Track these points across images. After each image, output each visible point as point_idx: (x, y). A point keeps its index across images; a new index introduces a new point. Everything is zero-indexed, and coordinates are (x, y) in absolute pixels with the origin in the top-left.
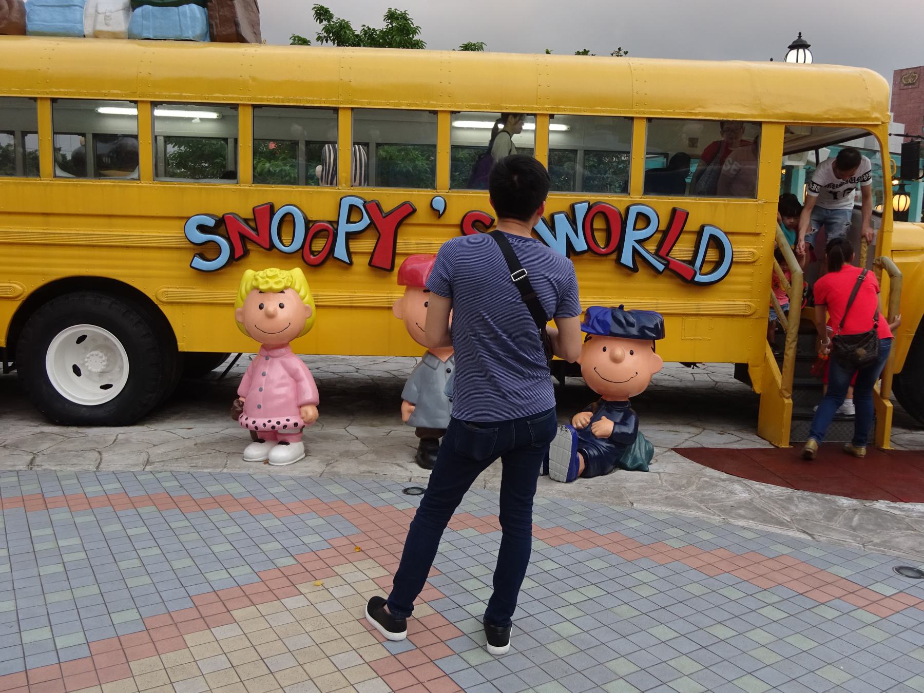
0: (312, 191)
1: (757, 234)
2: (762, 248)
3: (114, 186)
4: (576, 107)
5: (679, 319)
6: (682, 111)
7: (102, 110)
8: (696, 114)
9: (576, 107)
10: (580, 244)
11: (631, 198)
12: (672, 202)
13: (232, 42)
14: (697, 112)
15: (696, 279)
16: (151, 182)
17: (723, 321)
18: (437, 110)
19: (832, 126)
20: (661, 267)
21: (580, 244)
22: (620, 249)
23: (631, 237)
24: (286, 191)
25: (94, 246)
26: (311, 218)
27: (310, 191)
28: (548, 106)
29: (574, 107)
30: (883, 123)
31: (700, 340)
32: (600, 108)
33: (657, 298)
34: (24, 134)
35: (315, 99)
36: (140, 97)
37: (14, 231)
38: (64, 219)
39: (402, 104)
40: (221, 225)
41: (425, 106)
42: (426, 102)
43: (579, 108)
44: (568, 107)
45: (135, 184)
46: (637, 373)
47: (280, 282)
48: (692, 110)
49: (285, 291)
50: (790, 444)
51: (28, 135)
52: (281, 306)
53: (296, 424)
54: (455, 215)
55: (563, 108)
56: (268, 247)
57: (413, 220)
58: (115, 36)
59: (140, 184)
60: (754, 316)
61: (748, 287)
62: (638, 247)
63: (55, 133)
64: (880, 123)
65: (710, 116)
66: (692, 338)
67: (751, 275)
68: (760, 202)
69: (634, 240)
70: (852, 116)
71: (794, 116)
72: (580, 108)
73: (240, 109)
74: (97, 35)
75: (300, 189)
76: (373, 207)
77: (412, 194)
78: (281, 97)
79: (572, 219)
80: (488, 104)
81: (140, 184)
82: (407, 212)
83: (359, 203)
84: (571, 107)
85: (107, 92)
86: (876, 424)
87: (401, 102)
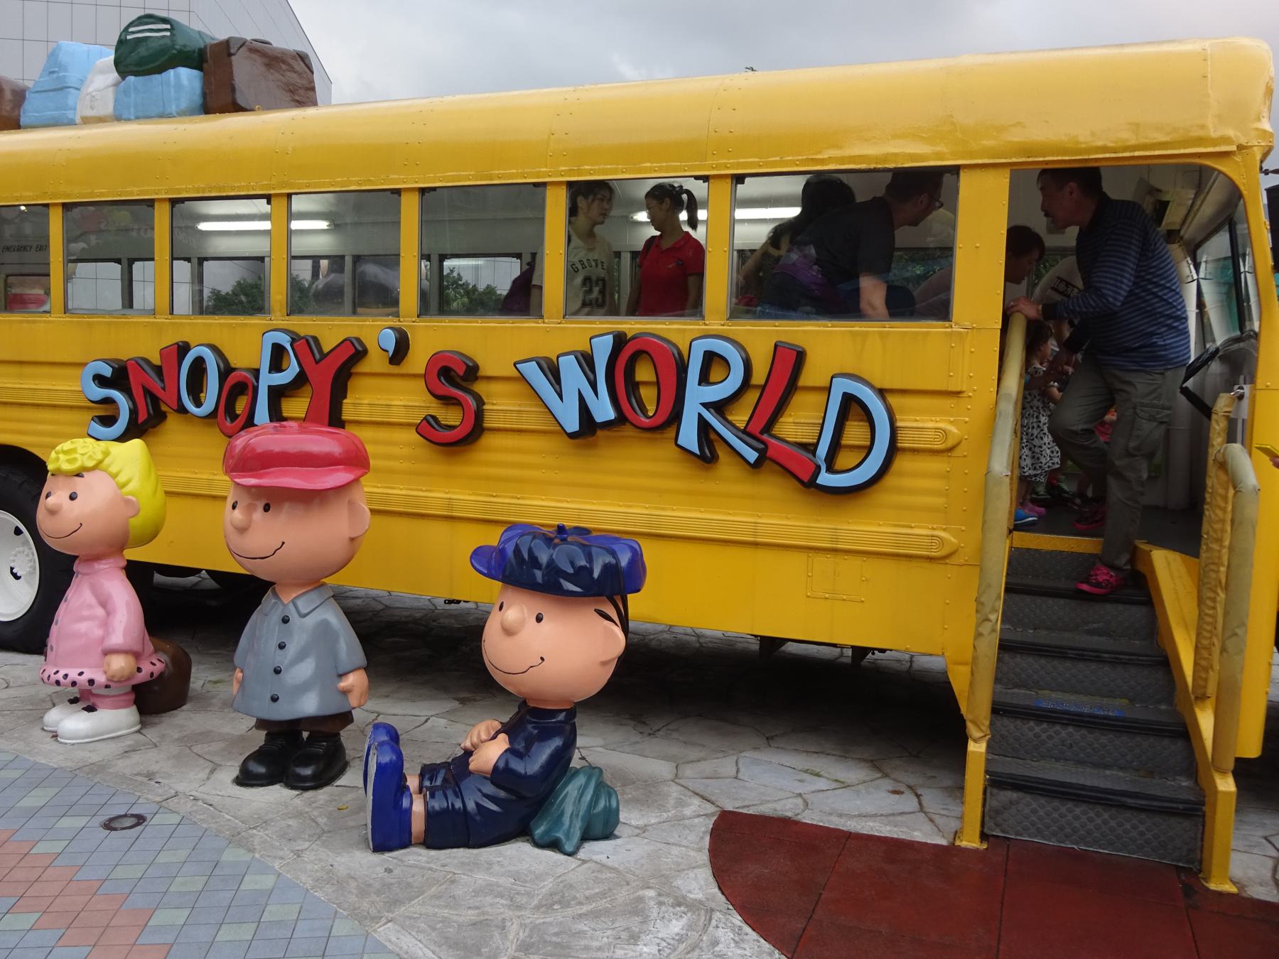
0: (235, 324)
1: (957, 394)
2: (966, 422)
3: (21, 322)
4: (609, 167)
5: (799, 559)
6: (796, 158)
7: (204, 226)
8: (822, 161)
9: (609, 167)
10: (603, 410)
11: (707, 325)
12: (777, 331)
13: (224, 113)
14: (826, 157)
15: (819, 481)
16: (60, 316)
17: (889, 565)
18: (400, 189)
19: (1141, 162)
20: (752, 456)
21: (603, 410)
22: (676, 417)
23: (697, 396)
24: (205, 324)
25: (54, 406)
26: (235, 364)
27: (232, 323)
28: (564, 168)
29: (606, 167)
30: (1240, 147)
31: (844, 600)
32: (649, 165)
33: (760, 514)
34: (131, 262)
35: (243, 184)
36: (51, 199)
37: (42, 387)
38: (46, 370)
39: (351, 183)
40: (119, 377)
41: (382, 184)
42: (383, 176)
43: (613, 166)
44: (597, 167)
45: (45, 319)
46: (542, 659)
47: (75, 459)
48: (816, 154)
49: (84, 473)
50: (984, 836)
51: (136, 263)
52: (73, 497)
53: (91, 682)
54: (418, 360)
55: (587, 169)
56: (176, 408)
57: (364, 367)
58: (101, 120)
59: (50, 319)
60: (954, 560)
61: (939, 501)
62: (710, 417)
63: (173, 258)
64: (1234, 148)
65: (849, 163)
66: (827, 596)
67: (946, 476)
68: (956, 329)
69: (701, 404)
70: (1162, 138)
71: (1026, 149)
72: (616, 166)
73: (157, 205)
74: (87, 121)
75: (222, 321)
76: (303, 345)
77: (363, 325)
78: (202, 186)
79: (587, 361)
80: (472, 173)
81: (50, 319)
82: (355, 353)
83: (285, 340)
84: (601, 167)
85: (18, 194)
86: (1204, 826)
87: (351, 179)
